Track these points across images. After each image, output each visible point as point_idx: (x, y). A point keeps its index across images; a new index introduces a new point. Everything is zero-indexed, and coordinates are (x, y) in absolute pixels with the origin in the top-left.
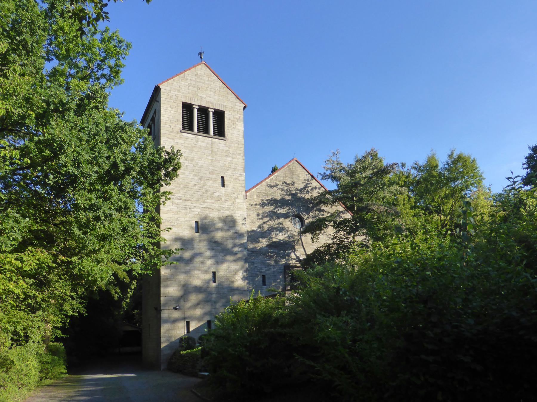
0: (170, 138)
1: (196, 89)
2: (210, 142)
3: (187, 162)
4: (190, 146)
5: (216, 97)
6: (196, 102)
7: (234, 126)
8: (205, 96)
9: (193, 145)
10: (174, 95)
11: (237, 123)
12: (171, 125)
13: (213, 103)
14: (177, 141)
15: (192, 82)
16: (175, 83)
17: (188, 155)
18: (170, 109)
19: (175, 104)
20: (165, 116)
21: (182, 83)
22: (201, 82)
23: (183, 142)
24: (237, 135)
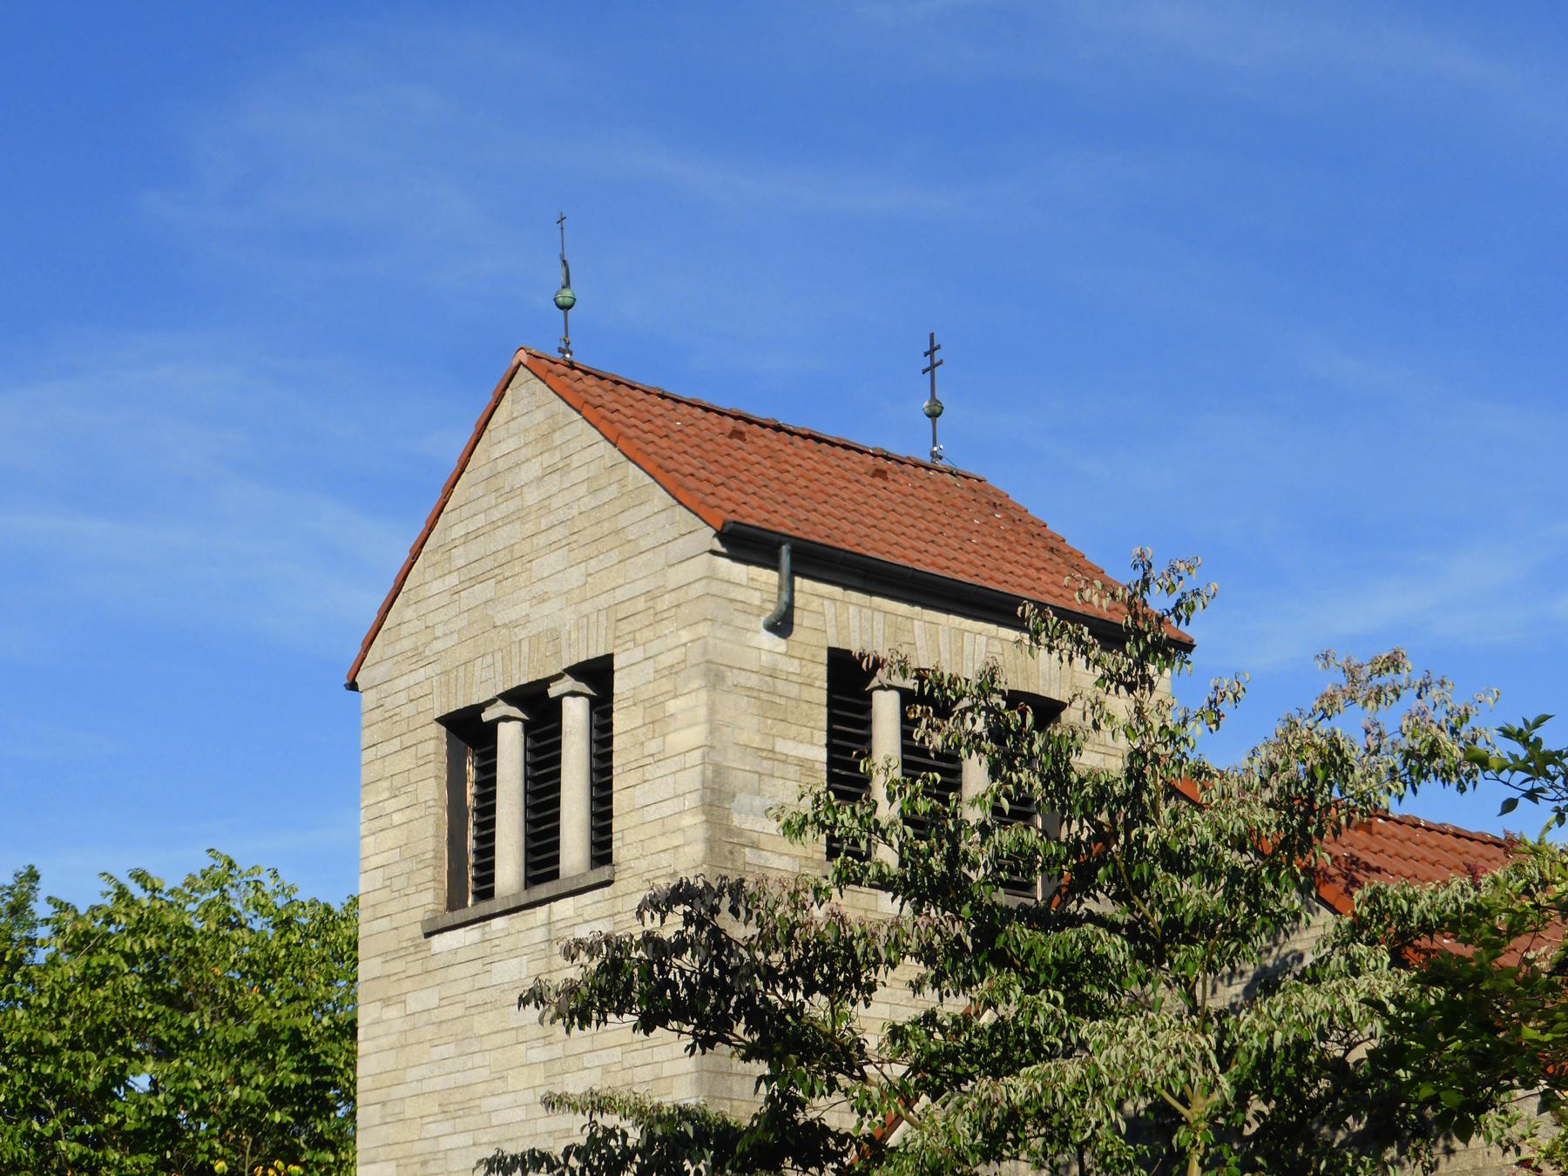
0: (386, 1002)
1: (484, 591)
2: (539, 935)
3: (446, 1127)
4: (458, 1010)
5: (575, 576)
6: (481, 685)
7: (653, 746)
8: (523, 609)
9: (474, 998)
10: (402, 698)
11: (672, 706)
12: (393, 907)
13: (554, 637)
14: (414, 1004)
15: (476, 549)
16: (409, 613)
17: (451, 1081)
18: (391, 805)
19: (406, 761)
20: (375, 861)
21: (436, 586)
22: (508, 519)
23: (430, 998)
24: (667, 809)
